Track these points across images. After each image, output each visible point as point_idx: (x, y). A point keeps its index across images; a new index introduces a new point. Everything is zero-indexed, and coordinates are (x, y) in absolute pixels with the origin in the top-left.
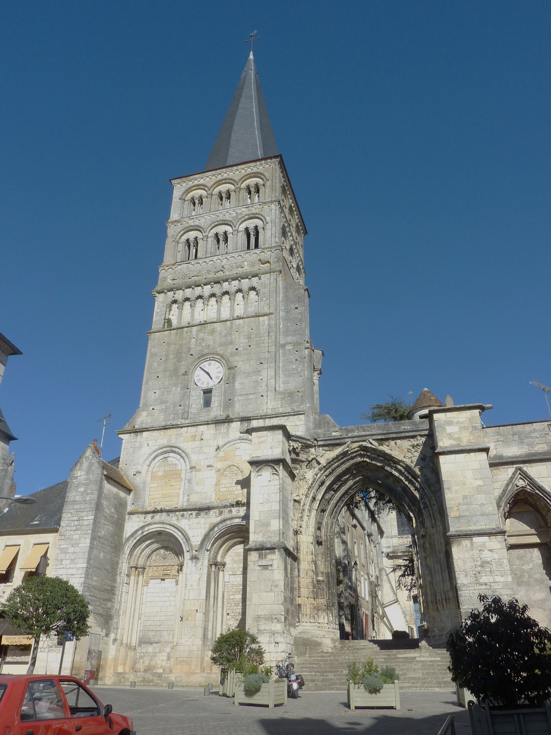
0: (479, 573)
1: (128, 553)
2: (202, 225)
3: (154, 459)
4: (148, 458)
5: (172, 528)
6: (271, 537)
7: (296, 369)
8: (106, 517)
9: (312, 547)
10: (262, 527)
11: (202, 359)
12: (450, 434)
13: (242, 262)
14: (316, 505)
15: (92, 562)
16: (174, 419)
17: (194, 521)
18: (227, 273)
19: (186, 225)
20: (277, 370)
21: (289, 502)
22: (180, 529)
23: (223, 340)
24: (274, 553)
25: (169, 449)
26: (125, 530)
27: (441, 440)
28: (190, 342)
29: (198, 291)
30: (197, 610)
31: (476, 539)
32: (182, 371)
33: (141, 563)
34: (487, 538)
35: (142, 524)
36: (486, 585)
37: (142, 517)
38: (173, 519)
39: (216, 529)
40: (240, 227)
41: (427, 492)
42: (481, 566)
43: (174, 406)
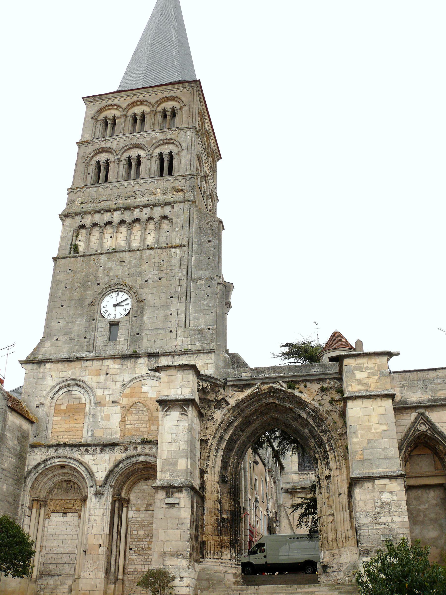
0: (379, 513)
1: (30, 485)
2: (114, 147)
3: (57, 391)
4: (51, 390)
5: (75, 462)
6: (178, 476)
7: (208, 305)
8: (9, 449)
9: (217, 486)
10: (170, 466)
11: (110, 289)
12: (358, 379)
13: (155, 188)
14: (223, 445)
16: (78, 351)
17: (98, 456)
19: (98, 147)
20: (188, 305)
21: (197, 442)
22: (84, 464)
23: (132, 270)
25: (72, 382)
26: (27, 462)
28: (97, 271)
29: (107, 217)
30: (100, 545)
31: (377, 482)
32: (88, 301)
33: (43, 495)
34: (388, 480)
35: (44, 457)
36: (384, 524)
37: (44, 450)
38: (77, 454)
39: (121, 465)
40: (154, 152)
41: (334, 435)
42: (381, 507)
43: (79, 338)
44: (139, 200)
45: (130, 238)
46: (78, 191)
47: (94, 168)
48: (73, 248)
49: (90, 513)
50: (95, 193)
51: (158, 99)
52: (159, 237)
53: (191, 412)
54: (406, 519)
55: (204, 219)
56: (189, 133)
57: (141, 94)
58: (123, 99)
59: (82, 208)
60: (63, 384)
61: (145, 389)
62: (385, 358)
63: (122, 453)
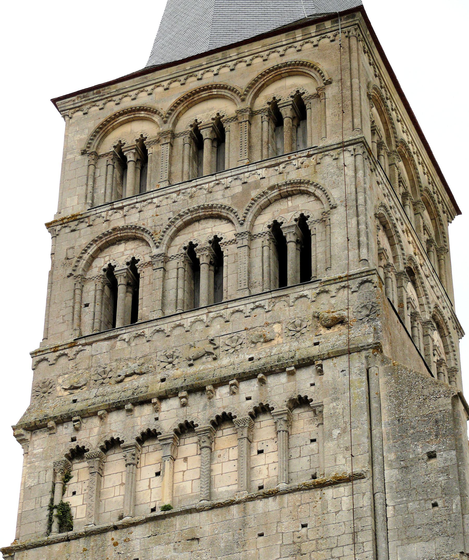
2: (149, 225)
13: (267, 324)
40: (257, 222)
45: (211, 470)
46: (59, 357)
47: (100, 287)
48: (57, 516)
50: (106, 356)
51: (254, 75)
52: (289, 459)
55: (410, 393)
56: (347, 158)
57: (207, 69)
58: (160, 89)
59: (75, 401)
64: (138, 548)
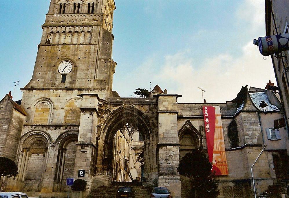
1: (23, 142)
5: (43, 133)
15: (6, 145)
17: (54, 131)
18: (78, 23)
20: (96, 70)
23: (73, 53)
24: (88, 147)
25: (44, 99)
27: (160, 107)
29: (63, 29)
30: (52, 168)
31: (168, 147)
32: (53, 65)
33: (28, 146)
35: (30, 130)
38: (45, 130)
42: (169, 157)
44: (78, 23)
49: (49, 154)
53: (95, 114)
54: (178, 162)
60: (41, 99)
61: (76, 104)
62: (176, 97)
63: (64, 130)
64: (60, 49)
